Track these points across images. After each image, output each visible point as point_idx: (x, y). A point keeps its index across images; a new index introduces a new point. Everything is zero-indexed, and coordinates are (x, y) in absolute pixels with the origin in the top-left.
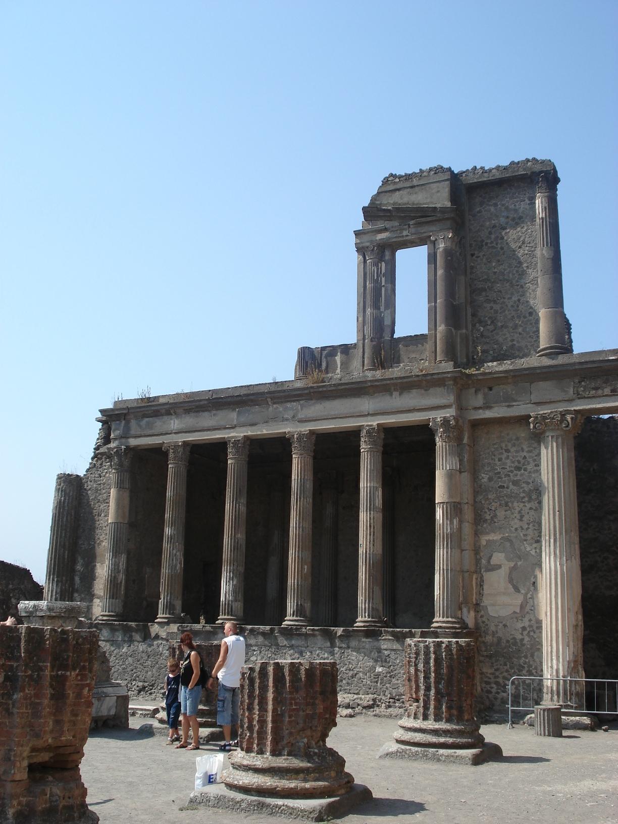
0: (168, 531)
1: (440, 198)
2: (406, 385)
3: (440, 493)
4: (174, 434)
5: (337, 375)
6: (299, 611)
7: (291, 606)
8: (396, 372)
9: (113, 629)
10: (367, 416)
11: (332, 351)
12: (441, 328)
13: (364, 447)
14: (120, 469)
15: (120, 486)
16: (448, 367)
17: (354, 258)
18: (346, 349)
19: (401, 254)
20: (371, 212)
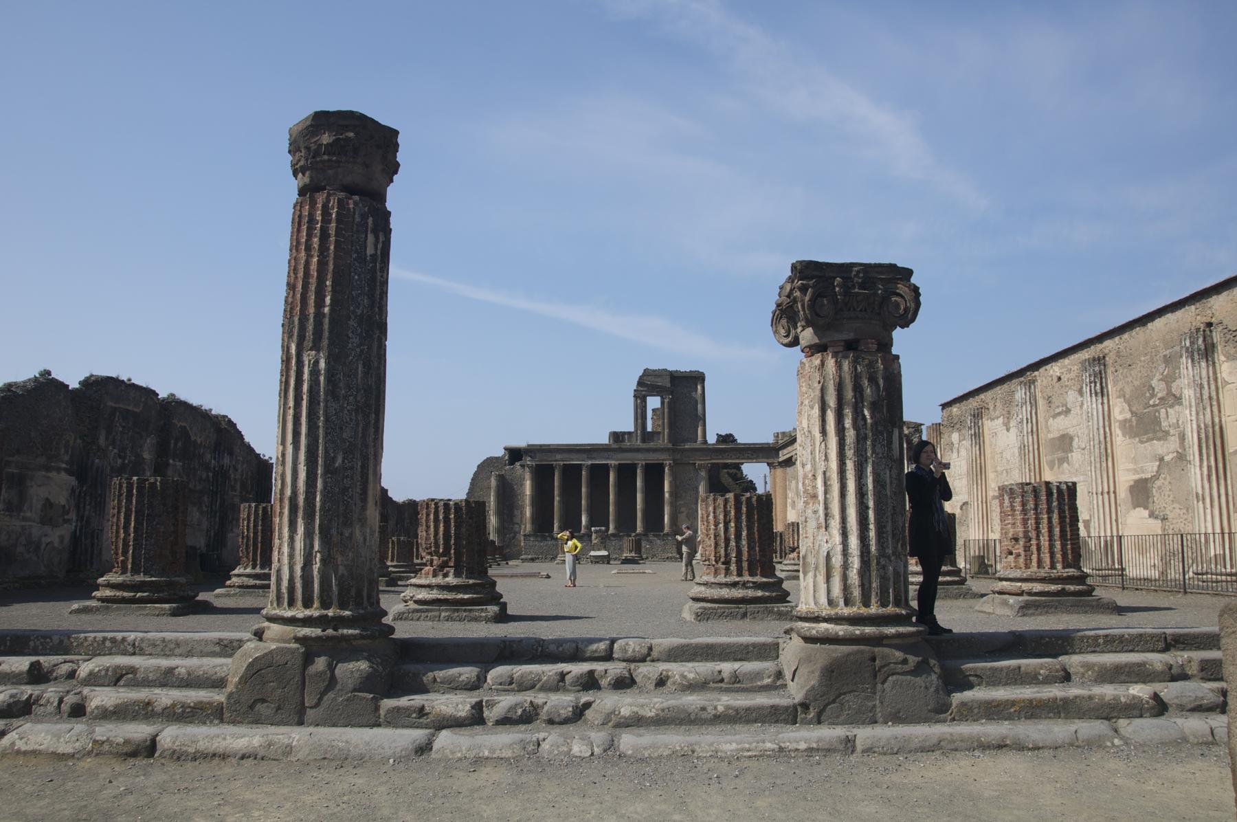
0: (557, 499)
1: (667, 383)
2: (655, 450)
3: (667, 488)
4: (559, 461)
5: (627, 444)
6: (616, 528)
7: (611, 526)
8: (651, 445)
9: (536, 536)
10: (641, 460)
11: (624, 433)
12: (666, 431)
13: (639, 471)
14: (531, 472)
15: (532, 480)
16: (670, 446)
17: (632, 399)
18: (630, 433)
19: (649, 398)
20: (640, 383)
